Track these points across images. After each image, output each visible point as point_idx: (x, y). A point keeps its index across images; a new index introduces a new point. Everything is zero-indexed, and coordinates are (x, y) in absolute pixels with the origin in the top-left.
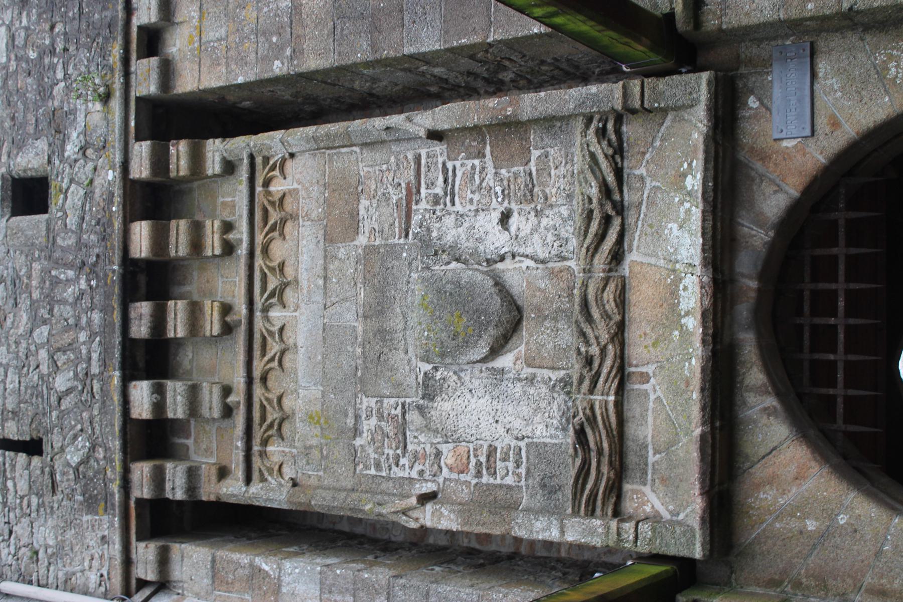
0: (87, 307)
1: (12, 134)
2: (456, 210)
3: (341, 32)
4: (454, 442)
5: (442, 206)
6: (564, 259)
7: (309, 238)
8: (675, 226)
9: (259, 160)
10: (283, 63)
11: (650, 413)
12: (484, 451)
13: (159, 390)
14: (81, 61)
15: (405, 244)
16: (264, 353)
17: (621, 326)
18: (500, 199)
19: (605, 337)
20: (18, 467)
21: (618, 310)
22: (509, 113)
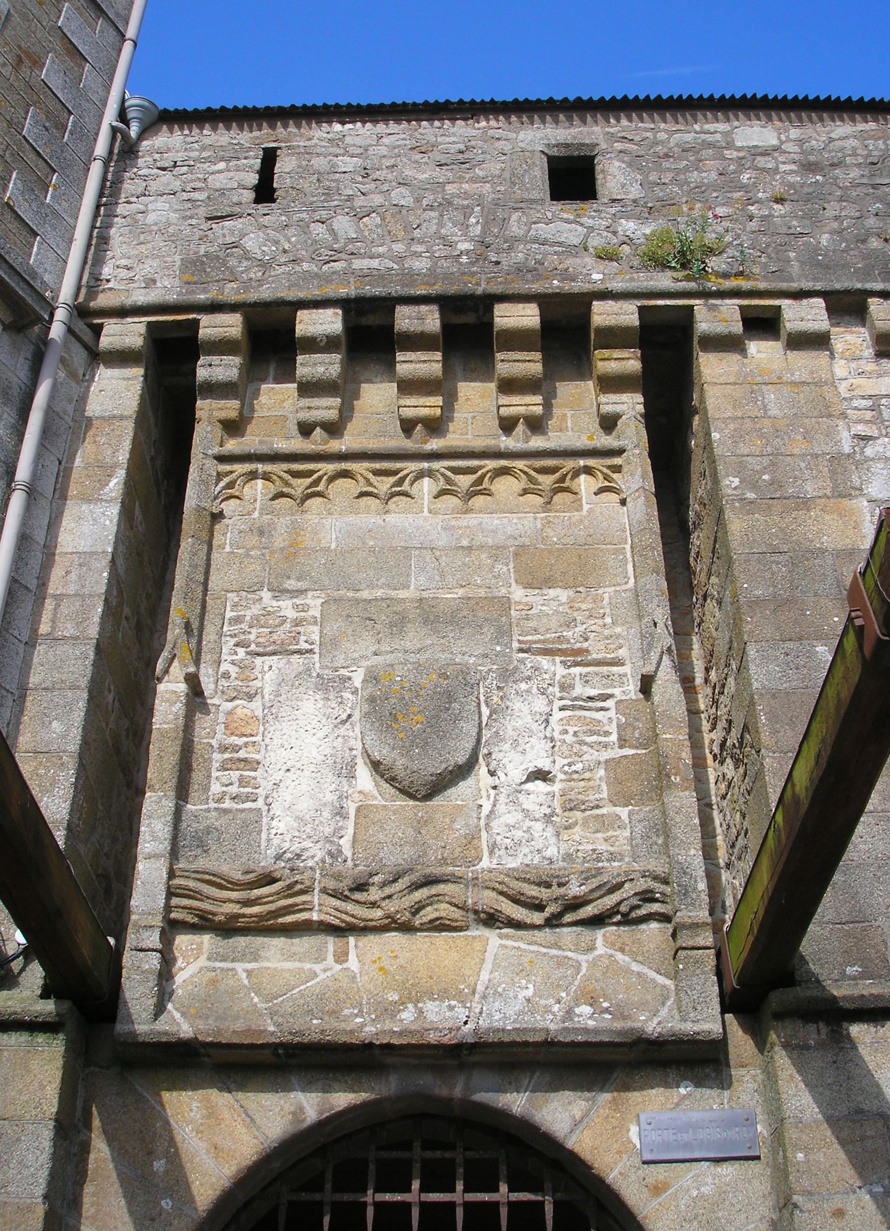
0: (435, 252)
1: (647, 154)
2: (554, 713)
3: (774, 562)
4: (264, 716)
5: (558, 695)
6: (491, 853)
7: (520, 526)
8: (530, 992)
9: (617, 461)
10: (735, 488)
11: (297, 964)
12: (251, 755)
13: (329, 344)
14: (738, 236)
15: (511, 648)
16: (377, 473)
17: (407, 928)
18: (566, 768)
19: (391, 907)
20: (242, 175)
21: (425, 923)
22: (673, 778)
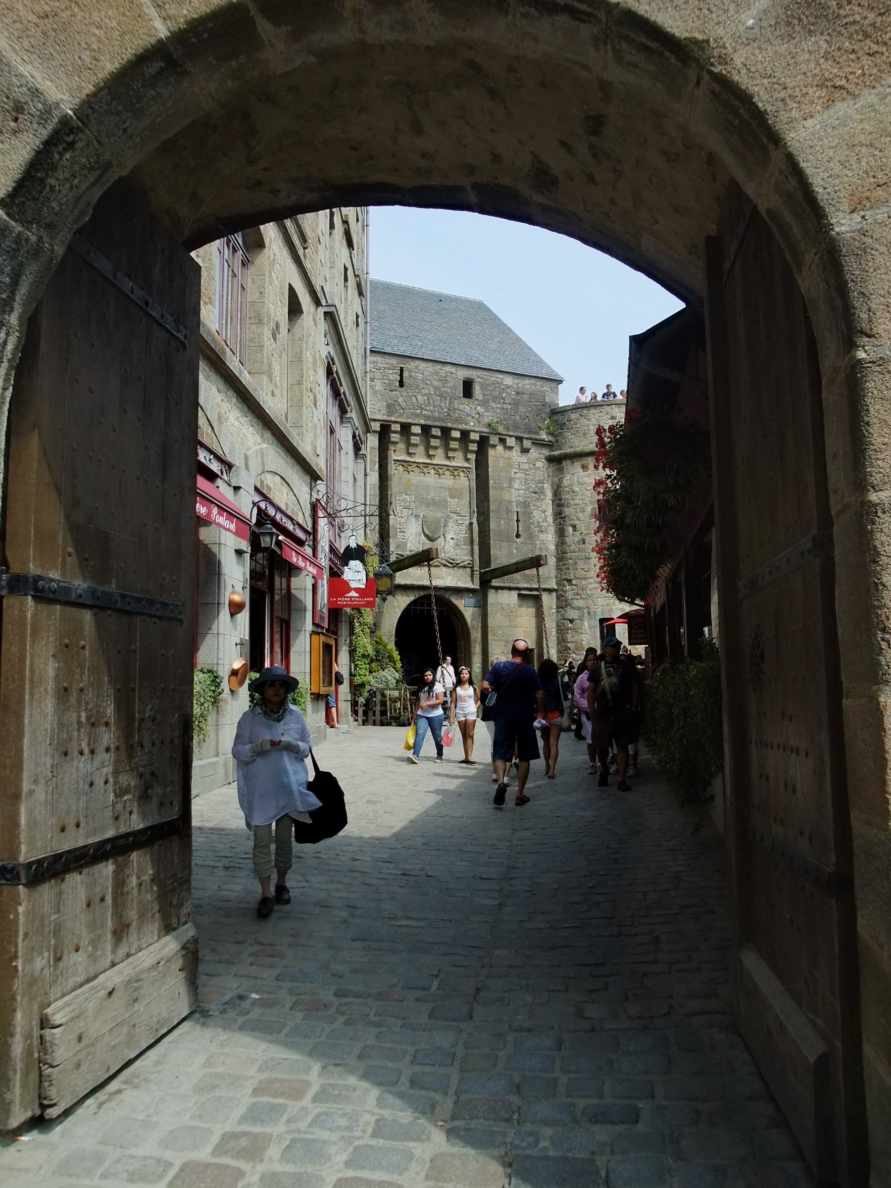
13: (417, 435)
